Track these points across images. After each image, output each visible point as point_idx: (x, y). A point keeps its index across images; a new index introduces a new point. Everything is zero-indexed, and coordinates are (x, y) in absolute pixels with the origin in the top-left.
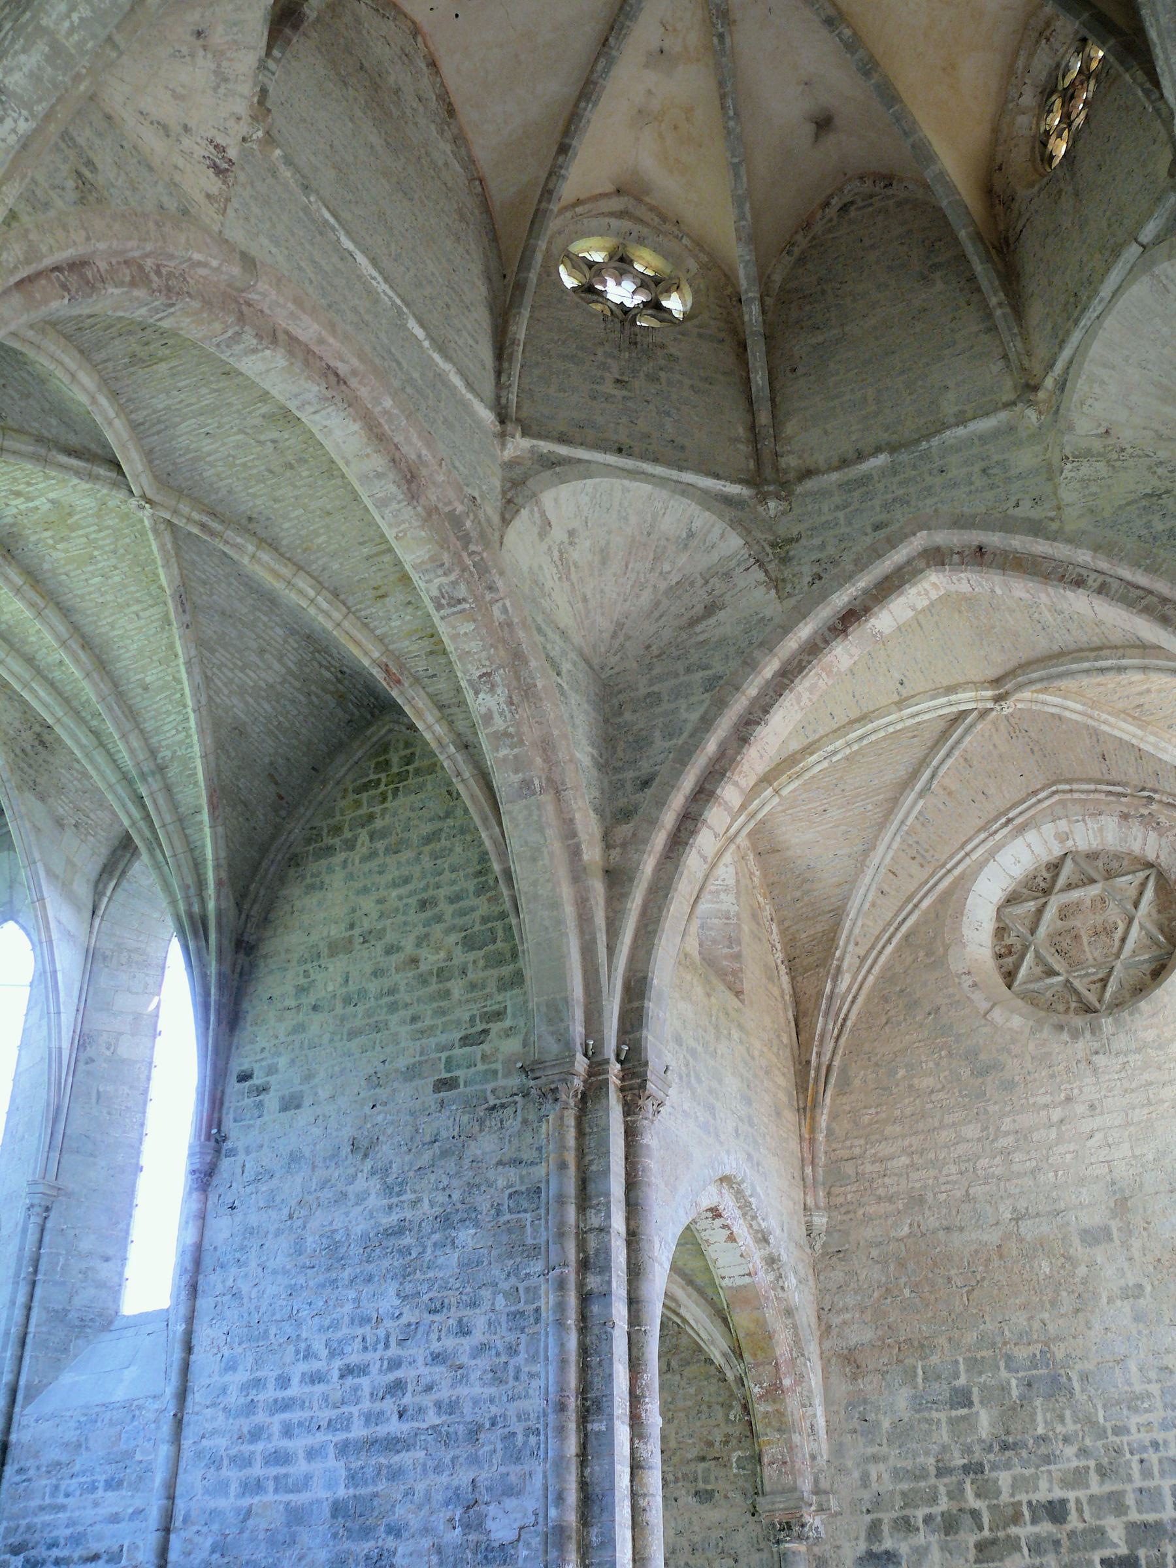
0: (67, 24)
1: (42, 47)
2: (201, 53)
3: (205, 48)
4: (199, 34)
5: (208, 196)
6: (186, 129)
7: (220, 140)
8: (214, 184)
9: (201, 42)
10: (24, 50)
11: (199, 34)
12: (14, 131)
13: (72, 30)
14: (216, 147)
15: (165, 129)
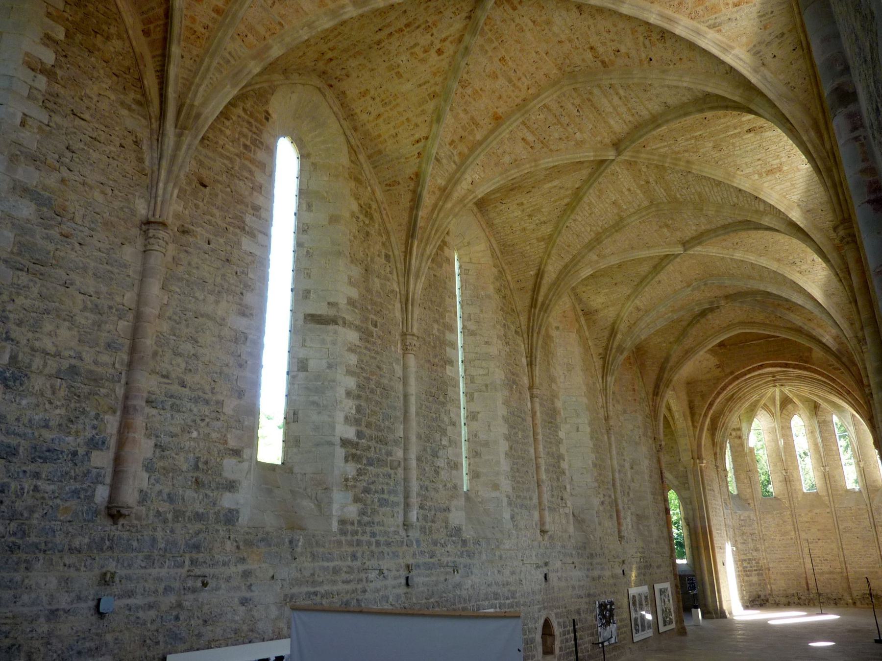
8: (720, 369)
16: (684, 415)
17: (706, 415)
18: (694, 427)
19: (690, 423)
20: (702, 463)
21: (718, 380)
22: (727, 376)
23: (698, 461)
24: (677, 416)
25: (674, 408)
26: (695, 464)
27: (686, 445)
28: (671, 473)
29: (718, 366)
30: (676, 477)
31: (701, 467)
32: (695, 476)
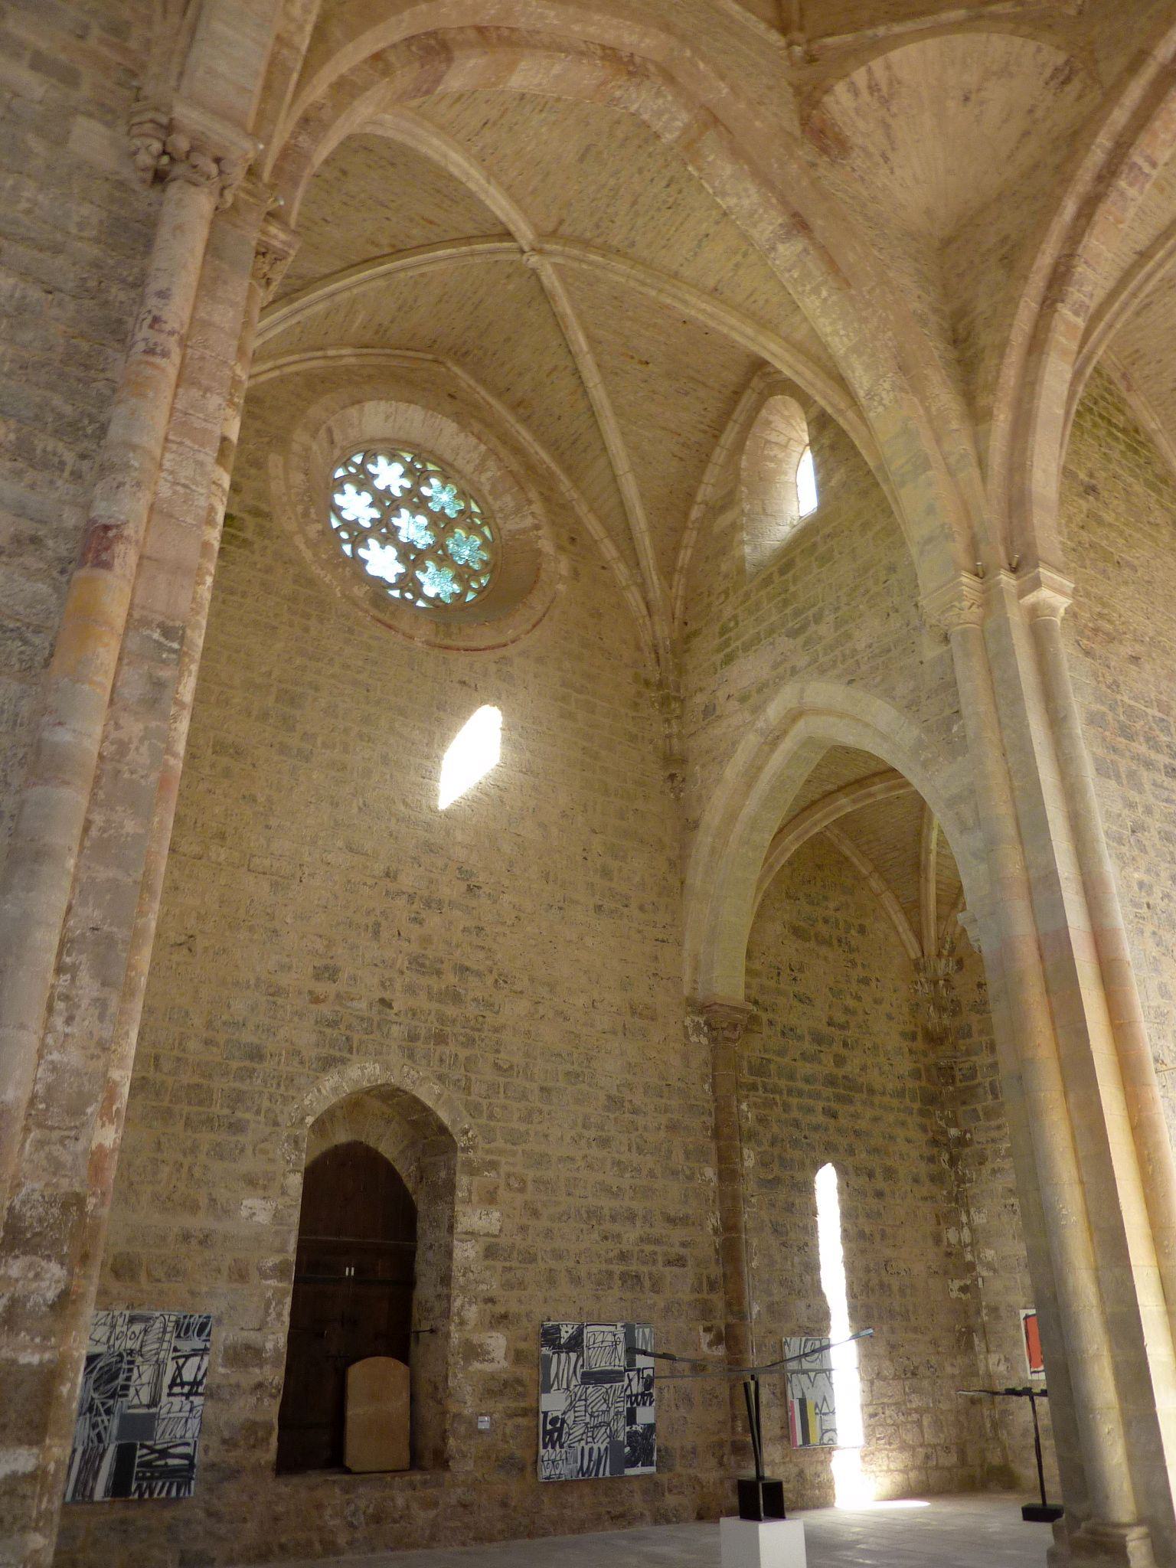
0: (845, 339)
1: (854, 359)
2: (983, 93)
3: (979, 90)
4: (967, 99)
5: (1080, 97)
6: (1031, 111)
7: (1048, 72)
8: (1075, 87)
9: (973, 97)
10: (853, 372)
11: (967, 99)
12: (888, 392)
13: (847, 336)
14: (1052, 78)
15: (1026, 134)
16: (902, 369)
17: (1037, 345)
18: (977, 415)
19: (945, 398)
20: (1037, 584)
21: (1075, 139)
22: (1112, 94)
23: (1005, 579)
24: (861, 379)
25: (839, 339)
26: (991, 599)
27: (930, 511)
28: (889, 694)
29: (1063, 77)
30: (912, 706)
31: (1034, 611)
32: (997, 663)
